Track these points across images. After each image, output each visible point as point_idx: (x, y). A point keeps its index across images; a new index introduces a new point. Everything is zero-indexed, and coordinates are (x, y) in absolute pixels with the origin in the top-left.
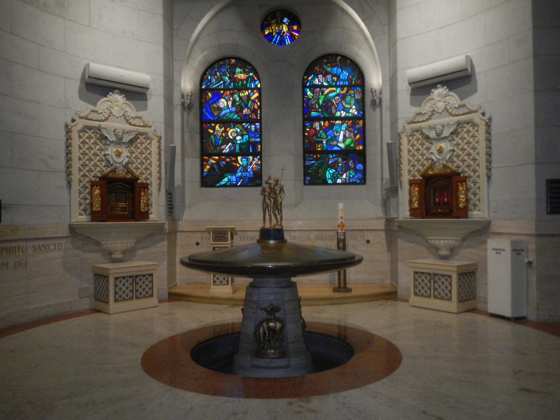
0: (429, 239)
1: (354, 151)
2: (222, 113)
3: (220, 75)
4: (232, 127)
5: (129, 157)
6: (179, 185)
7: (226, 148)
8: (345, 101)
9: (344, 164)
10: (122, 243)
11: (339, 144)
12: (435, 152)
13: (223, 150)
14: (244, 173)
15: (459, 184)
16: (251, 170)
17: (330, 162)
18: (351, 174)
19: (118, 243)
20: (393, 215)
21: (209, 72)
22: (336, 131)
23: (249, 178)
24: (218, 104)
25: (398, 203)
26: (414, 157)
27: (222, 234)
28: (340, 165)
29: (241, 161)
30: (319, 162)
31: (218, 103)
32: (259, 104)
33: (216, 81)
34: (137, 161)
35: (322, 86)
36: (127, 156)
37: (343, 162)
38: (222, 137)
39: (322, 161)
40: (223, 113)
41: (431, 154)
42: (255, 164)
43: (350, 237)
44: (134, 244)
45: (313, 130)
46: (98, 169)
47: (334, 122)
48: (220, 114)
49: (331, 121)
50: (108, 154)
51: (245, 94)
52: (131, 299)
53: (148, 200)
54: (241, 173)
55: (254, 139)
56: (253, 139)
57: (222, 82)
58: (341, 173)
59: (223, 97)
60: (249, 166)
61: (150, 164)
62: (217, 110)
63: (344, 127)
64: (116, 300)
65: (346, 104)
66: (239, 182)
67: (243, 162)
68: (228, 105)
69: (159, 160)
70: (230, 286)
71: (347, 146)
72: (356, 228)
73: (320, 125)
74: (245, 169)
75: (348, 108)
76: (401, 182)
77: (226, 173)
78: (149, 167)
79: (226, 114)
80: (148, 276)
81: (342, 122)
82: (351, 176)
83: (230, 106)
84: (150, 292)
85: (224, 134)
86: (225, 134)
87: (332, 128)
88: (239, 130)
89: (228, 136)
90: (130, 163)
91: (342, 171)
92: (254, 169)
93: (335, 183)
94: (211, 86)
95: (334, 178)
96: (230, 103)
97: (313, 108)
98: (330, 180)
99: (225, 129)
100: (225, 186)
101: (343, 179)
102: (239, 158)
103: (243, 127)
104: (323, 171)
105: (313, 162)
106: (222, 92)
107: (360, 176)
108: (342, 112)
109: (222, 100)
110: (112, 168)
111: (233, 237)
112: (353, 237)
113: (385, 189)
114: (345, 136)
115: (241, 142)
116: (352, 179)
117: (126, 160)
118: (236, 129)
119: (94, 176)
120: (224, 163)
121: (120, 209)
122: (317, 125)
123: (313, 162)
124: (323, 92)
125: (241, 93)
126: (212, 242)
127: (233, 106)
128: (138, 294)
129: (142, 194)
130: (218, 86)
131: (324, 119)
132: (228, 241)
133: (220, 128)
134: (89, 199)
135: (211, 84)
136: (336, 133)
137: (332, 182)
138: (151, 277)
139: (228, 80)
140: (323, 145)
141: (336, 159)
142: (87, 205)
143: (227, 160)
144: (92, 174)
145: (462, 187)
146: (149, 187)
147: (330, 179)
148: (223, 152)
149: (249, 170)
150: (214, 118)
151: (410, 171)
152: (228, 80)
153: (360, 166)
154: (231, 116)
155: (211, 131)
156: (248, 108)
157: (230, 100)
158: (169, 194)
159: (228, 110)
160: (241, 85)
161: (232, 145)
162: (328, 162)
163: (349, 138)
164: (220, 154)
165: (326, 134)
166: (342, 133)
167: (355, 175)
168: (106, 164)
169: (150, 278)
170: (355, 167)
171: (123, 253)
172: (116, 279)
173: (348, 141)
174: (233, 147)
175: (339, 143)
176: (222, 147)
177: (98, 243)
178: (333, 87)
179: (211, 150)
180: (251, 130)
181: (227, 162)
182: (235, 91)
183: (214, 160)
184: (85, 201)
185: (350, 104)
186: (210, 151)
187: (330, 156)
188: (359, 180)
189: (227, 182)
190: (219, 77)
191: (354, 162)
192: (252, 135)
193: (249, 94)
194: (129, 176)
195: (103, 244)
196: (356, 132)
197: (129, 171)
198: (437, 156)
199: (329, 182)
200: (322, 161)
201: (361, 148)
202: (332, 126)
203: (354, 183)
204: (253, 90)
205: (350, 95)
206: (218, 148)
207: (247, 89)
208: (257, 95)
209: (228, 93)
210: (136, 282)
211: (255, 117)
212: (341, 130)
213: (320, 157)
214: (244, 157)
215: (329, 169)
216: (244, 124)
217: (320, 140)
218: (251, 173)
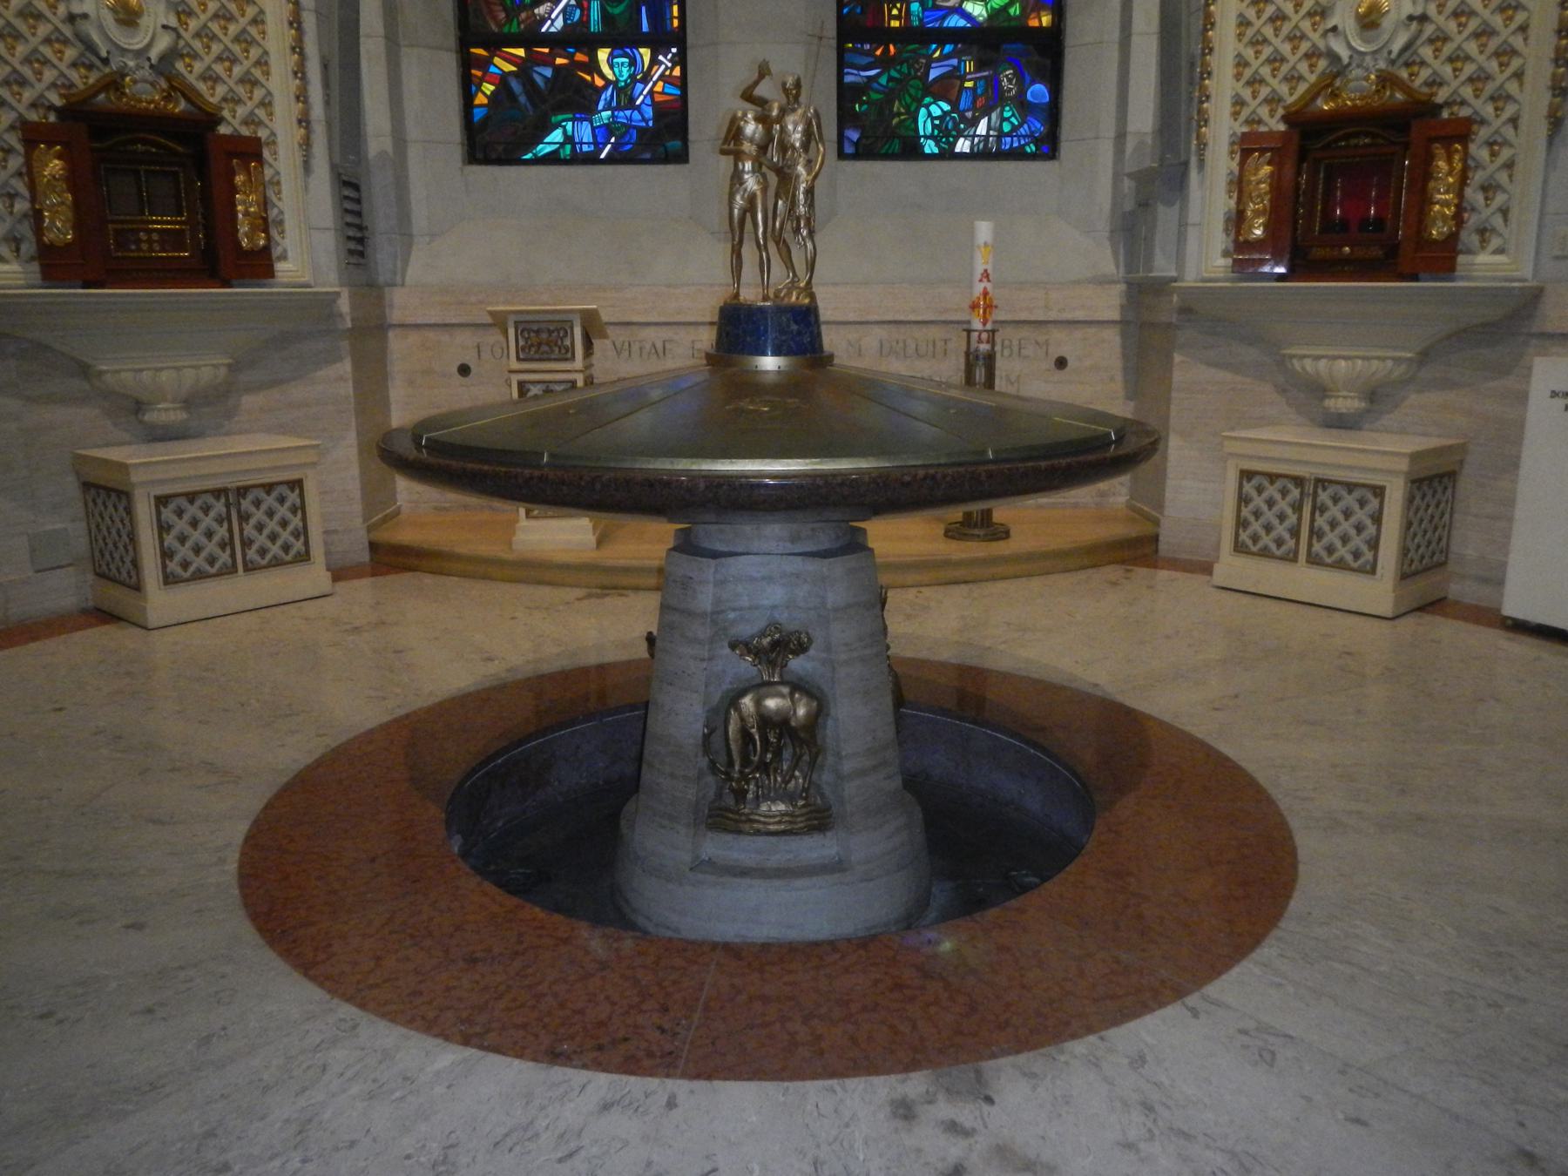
0: (1292, 357)
1: (1021, 33)
5: (174, 30)
6: (383, 154)
7: (553, 16)
9: (982, 83)
10: (177, 369)
12: (1349, 25)
13: (543, 21)
14: (621, 114)
15: (1438, 149)
16: (648, 101)
17: (933, 74)
18: (1007, 119)
19: (161, 369)
20: (1162, 267)
23: (642, 132)
25: (1183, 225)
26: (1260, 48)
27: (550, 332)
28: (969, 84)
29: (612, 67)
30: (894, 74)
34: (209, 47)
36: (164, 27)
37: (978, 75)
39: (905, 69)
41: (1330, 34)
42: (662, 77)
44: (223, 371)
46: (49, 75)
50: (85, 16)
52: (230, 570)
53: (265, 204)
54: (609, 113)
58: (969, 114)
60: (639, 86)
61: (262, 63)
64: (169, 580)
67: (616, 70)
69: (298, 48)
72: (1023, 316)
74: (625, 98)
76: (1202, 146)
77: (560, 108)
78: (257, 73)
80: (284, 490)
82: (1007, 128)
84: (298, 546)
90: (182, 56)
91: (974, 108)
92: (658, 98)
93: (948, 154)
98: (931, 143)
100: (552, 159)
101: (976, 140)
102: (603, 54)
104: (907, 107)
105: (872, 73)
107: (1039, 127)
110: (107, 70)
111: (592, 344)
112: (1010, 347)
113: (1130, 175)
116: (1008, 139)
117: (163, 43)
119: (34, 105)
120: (548, 72)
121: (155, 237)
123: (872, 73)
126: (515, 365)
128: (252, 554)
129: (239, 179)
134: (23, 197)
137: (936, 150)
138: (297, 491)
141: (954, 62)
142: (20, 221)
143: (559, 61)
144: (28, 95)
145: (1449, 161)
146: (266, 154)
147: (931, 137)
148: (543, 30)
149: (638, 102)
151: (1239, 102)
153: (1038, 92)
158: (347, 184)
162: (927, 74)
164: (531, 38)
167: (1021, 125)
168: (82, 55)
169: (293, 497)
170: (1022, 93)
171: (188, 403)
172: (161, 501)
174: (578, 12)
176: (536, 11)
177: (84, 371)
179: (494, 18)
183: (510, 59)
184: (12, 206)
186: (494, 28)
187: (935, 51)
188: (1037, 142)
189: (562, 145)
191: (1019, 74)
194: (182, 106)
195: (101, 373)
197: (177, 87)
198: (1353, 44)
199: (927, 150)
200: (905, 69)
201: (1046, 20)
203: (1017, 155)
206: (523, 15)
210: (239, 511)
213: (898, 52)
214: (620, 52)
215: (928, 100)
218: (649, 112)
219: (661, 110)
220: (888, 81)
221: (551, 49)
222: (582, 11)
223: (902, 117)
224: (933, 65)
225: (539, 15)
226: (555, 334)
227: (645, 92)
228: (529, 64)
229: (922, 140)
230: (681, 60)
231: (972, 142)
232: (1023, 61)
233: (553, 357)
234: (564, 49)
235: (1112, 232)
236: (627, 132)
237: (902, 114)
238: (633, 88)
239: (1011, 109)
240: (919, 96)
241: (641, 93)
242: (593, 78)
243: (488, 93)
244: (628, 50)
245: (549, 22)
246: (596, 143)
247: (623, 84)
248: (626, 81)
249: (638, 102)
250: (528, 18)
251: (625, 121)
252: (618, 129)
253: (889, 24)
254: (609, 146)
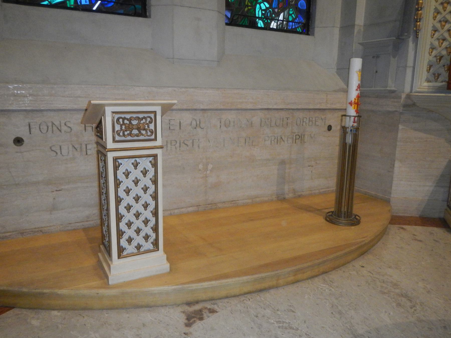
18: (291, 15)
43: (307, 122)
58: (276, 10)
70: (161, 253)
82: (290, 19)
91: (278, 8)
93: (267, 28)
98: (261, 22)
116: (291, 23)
132: (155, 139)
137: (263, 26)
167: (296, 19)
203: (293, 31)
223: (249, 8)
226: (144, 120)
229: (257, 20)
233: (141, 137)
235: (337, 69)
239: (292, 10)
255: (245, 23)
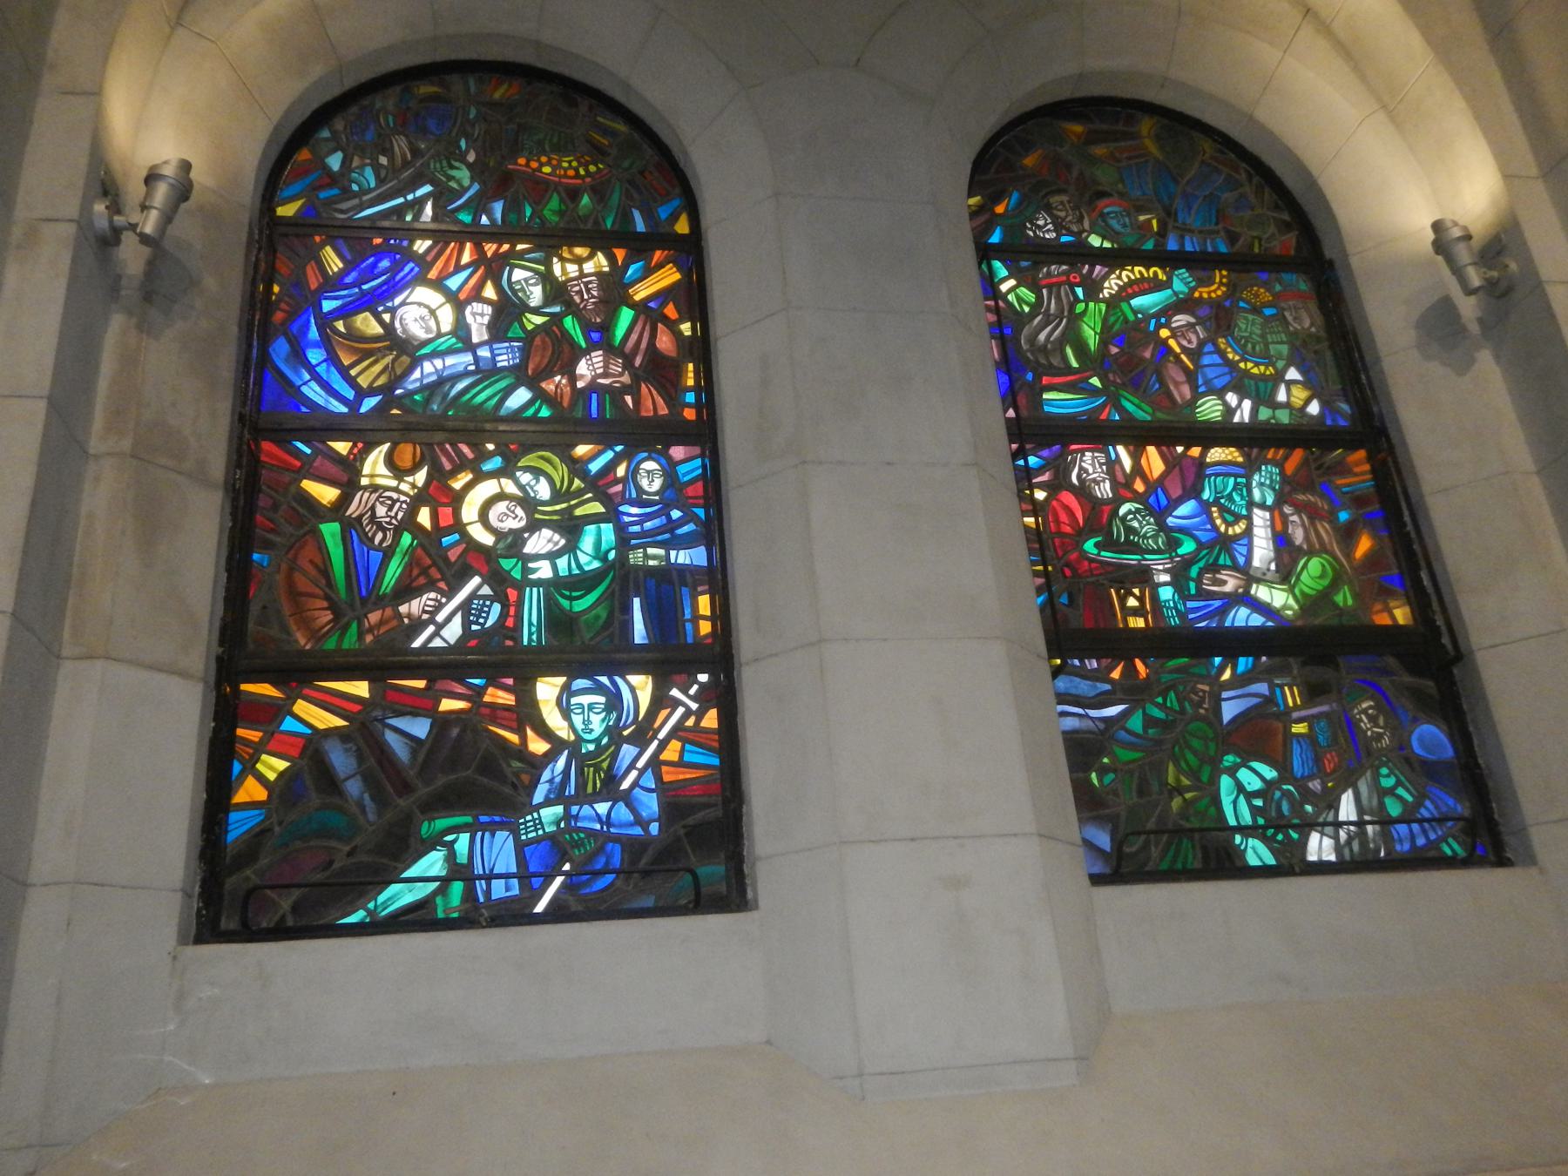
2: (417, 374)
3: (416, 153)
4: (496, 462)
7: (440, 618)
8: (1238, 342)
11: (1262, 592)
13: (417, 626)
14: (586, 810)
17: (1229, 710)
18: (1391, 792)
21: (334, 133)
22: (1223, 510)
23: (634, 847)
24: (387, 317)
29: (566, 713)
31: (393, 311)
32: (686, 328)
33: (381, 181)
35: (1079, 254)
38: (406, 539)
40: (429, 370)
42: (674, 733)
45: (1068, 498)
47: (1195, 451)
48: (398, 379)
49: (1180, 449)
51: (589, 267)
54: (559, 809)
55: (661, 552)
56: (651, 551)
57: (427, 189)
58: (1315, 785)
59: (433, 274)
60: (628, 751)
62: (390, 349)
63: (1263, 486)
65: (1245, 360)
66: (549, 879)
67: (577, 720)
68: (461, 330)
71: (1313, 604)
73: (1112, 465)
75: (1262, 377)
79: (444, 381)
81: (1247, 456)
82: (1394, 809)
83: (478, 334)
85: (424, 517)
86: (435, 517)
87: (1193, 492)
88: (543, 490)
89: (459, 527)
91: (1319, 771)
92: (669, 775)
93: (1291, 864)
94: (344, 206)
95: (1281, 825)
96: (479, 318)
97: (1052, 370)
99: (439, 477)
100: (417, 919)
102: (547, 689)
103: (577, 467)
104: (1194, 774)
106: (421, 246)
108: (1232, 398)
109: (423, 294)
114: (1281, 540)
115: (563, 571)
118: (525, 478)
122: (1089, 464)
124: (1093, 290)
125: (562, 259)
127: (498, 330)
130: (399, 212)
131: (1138, 437)
133: (399, 472)
135: (347, 194)
136: (1228, 524)
139: (466, 182)
140: (1155, 598)
141: (1262, 688)
143: (447, 705)
148: (417, 644)
149: (625, 785)
150: (354, 405)
152: (466, 182)
154: (484, 396)
155: (326, 494)
156: (611, 350)
157: (477, 296)
159: (469, 358)
160: (554, 212)
161: (486, 590)
163: (1311, 553)
165: (1162, 526)
166: (1260, 518)
167: (1418, 804)
170: (1402, 746)
173: (1312, 572)
174: (497, 608)
175: (1259, 581)
176: (403, 609)
178: (1147, 260)
179: (306, 623)
180: (640, 490)
181: (443, 723)
182: (520, 247)
183: (330, 703)
185: (1269, 360)
186: (302, 640)
187: (1221, 670)
189: (445, 882)
190: (406, 164)
192: (648, 525)
193: (617, 270)
196: (1343, 516)
202: (1191, 479)
204: (640, 246)
205: (1256, 310)
206: (374, 617)
207: (599, 240)
208: (669, 276)
209: (466, 258)
211: (663, 410)
212: (1251, 504)
213: (1154, 672)
215: (1230, 759)
216: (581, 450)
217: (1132, 559)
218: (650, 804)
219: (675, 803)
220: (1146, 727)
221: (431, 681)
222: (505, 606)
223: (1188, 796)
224: (1225, 695)
225: (409, 616)
227: (640, 764)
228: (378, 713)
230: (724, 696)
231: (1336, 838)
232: (1384, 682)
234: (461, 681)
236: (600, 850)
237: (1189, 789)
238: (614, 756)
240: (1212, 753)
241: (632, 766)
242: (524, 739)
243: (272, 776)
244: (604, 680)
245: (431, 629)
246: (524, 875)
247: (591, 747)
248: (597, 741)
249: (625, 785)
250: (381, 622)
251: (598, 827)
252: (578, 844)
253: (1125, 621)
254: (559, 880)
255: (1185, 863)
